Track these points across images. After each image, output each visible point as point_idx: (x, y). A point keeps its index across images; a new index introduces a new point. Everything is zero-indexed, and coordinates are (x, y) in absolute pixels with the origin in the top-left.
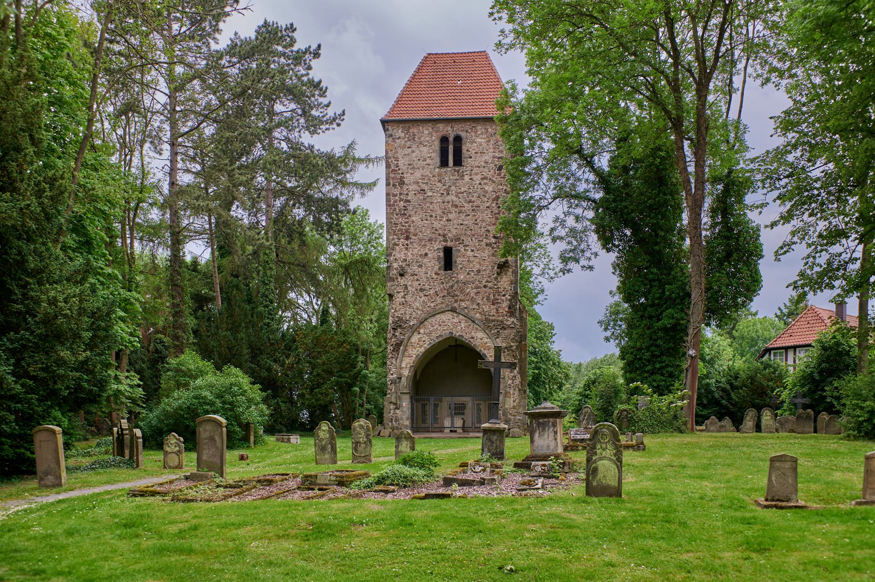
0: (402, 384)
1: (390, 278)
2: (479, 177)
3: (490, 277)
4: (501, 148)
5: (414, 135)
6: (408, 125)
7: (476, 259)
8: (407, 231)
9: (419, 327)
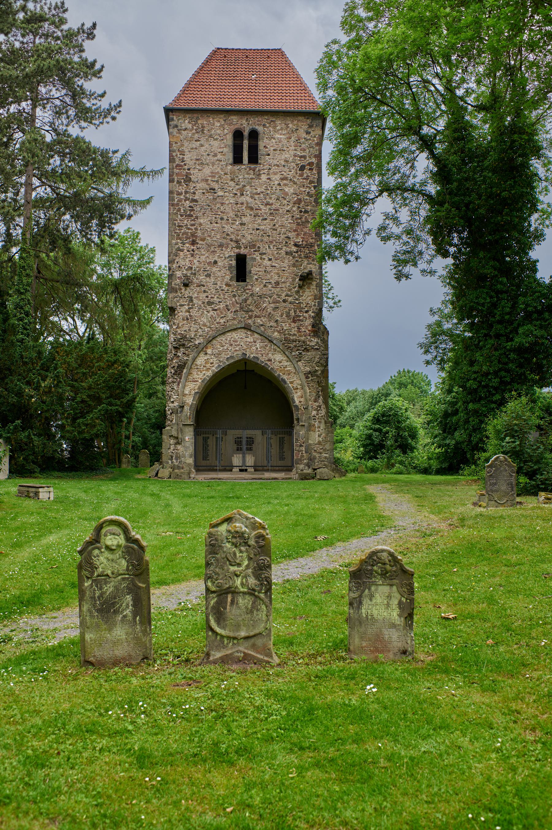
0: (184, 414)
1: (173, 288)
2: (278, 177)
3: (290, 290)
5: (203, 127)
6: (196, 115)
7: (272, 270)
8: (193, 235)
9: (206, 347)
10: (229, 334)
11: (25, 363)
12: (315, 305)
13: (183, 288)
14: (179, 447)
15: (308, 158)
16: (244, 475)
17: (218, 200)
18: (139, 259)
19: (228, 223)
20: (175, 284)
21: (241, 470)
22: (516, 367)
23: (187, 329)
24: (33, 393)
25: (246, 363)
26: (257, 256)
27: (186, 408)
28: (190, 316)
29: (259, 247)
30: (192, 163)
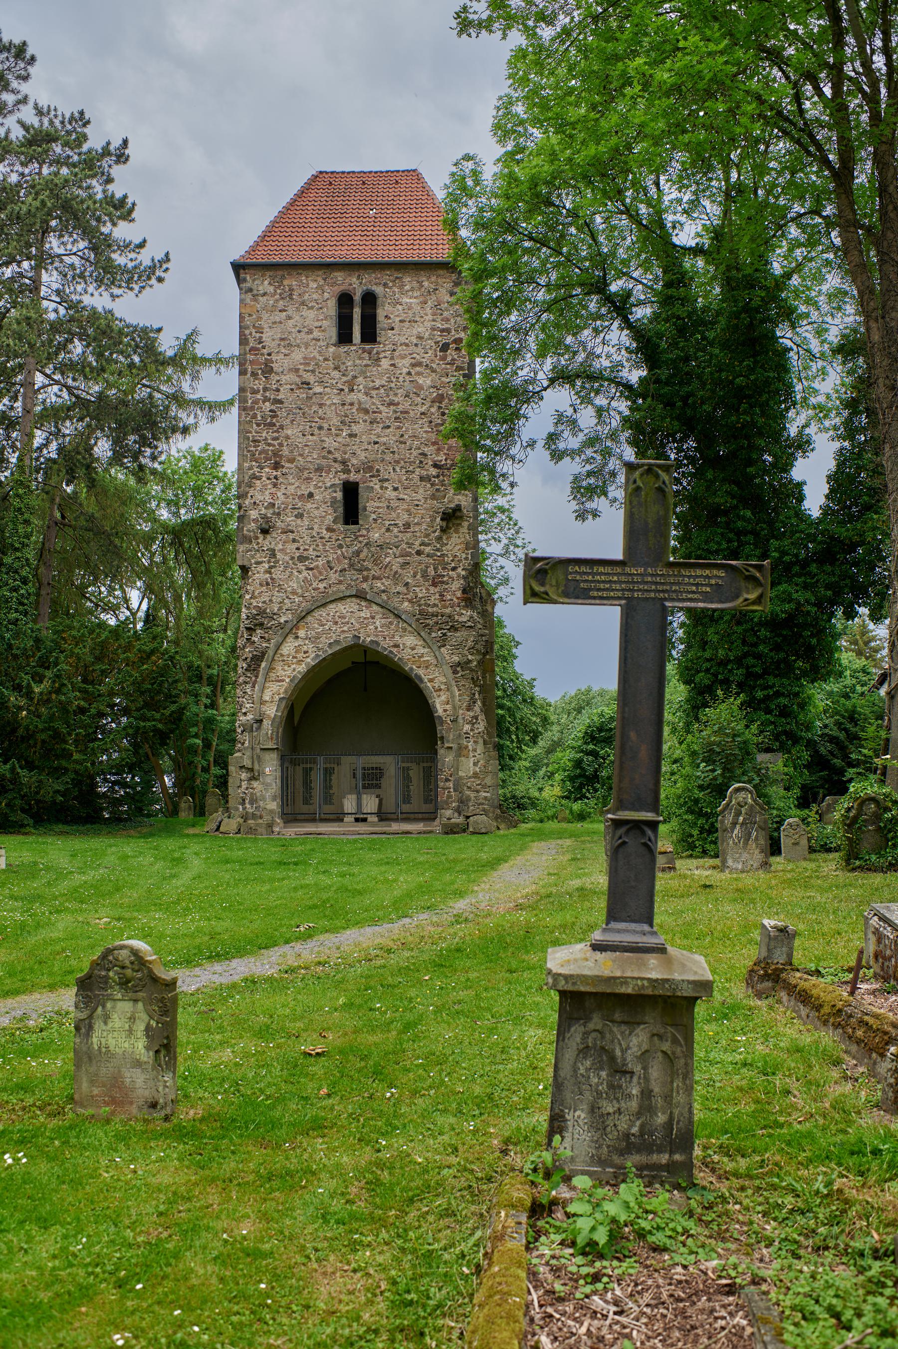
0: (263, 732)
1: (245, 537)
2: (407, 362)
3: (427, 536)
4: (446, 314)
5: (291, 290)
6: (280, 273)
7: (400, 505)
8: (276, 454)
9: (296, 626)
10: (331, 606)
11: (16, 657)
12: (466, 559)
13: (261, 537)
14: (255, 784)
15: (453, 332)
16: (361, 827)
17: (314, 400)
18: (223, 492)
19: (328, 436)
20: (249, 531)
21: (357, 820)
22: (771, 650)
23: (267, 599)
24: (23, 702)
25: (365, 651)
26: (375, 484)
27: (266, 723)
28: (272, 579)
29: (378, 471)
30: (274, 344)
